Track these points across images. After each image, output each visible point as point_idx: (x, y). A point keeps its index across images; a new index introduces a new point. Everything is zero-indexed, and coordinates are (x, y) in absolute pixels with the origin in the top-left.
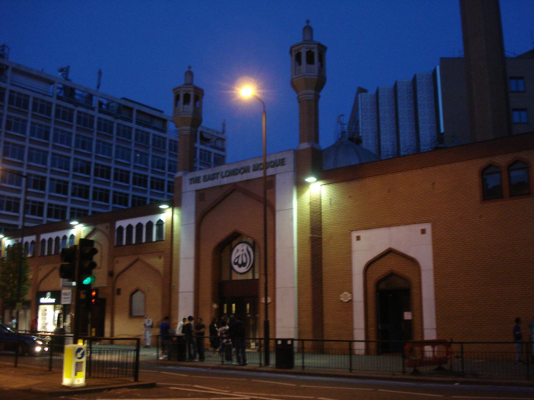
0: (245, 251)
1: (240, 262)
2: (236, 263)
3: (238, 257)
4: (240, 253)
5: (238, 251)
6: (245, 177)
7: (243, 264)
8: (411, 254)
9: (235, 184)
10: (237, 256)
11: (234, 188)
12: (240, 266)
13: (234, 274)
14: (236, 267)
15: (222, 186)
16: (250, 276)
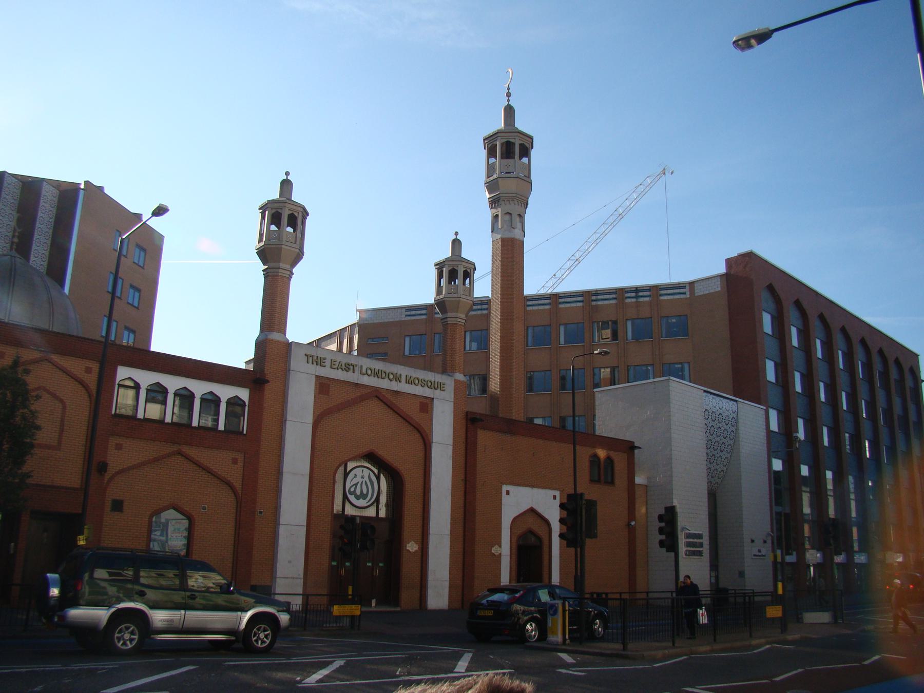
0: (366, 479)
1: (358, 492)
2: (354, 493)
3: (356, 485)
4: (359, 479)
5: (355, 476)
6: (394, 386)
7: (363, 496)
8: (547, 517)
9: (377, 390)
10: (354, 482)
11: (377, 394)
12: (358, 498)
13: (347, 505)
14: (352, 498)
15: (357, 385)
16: (371, 512)
